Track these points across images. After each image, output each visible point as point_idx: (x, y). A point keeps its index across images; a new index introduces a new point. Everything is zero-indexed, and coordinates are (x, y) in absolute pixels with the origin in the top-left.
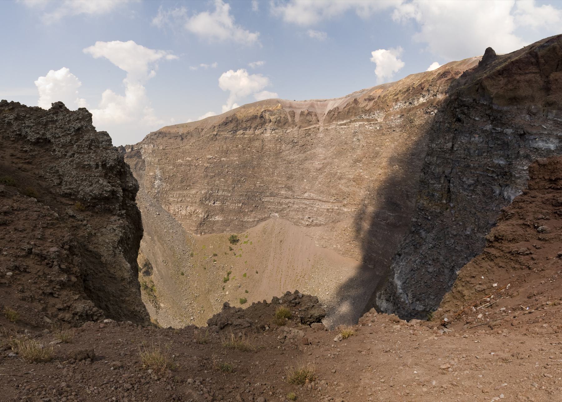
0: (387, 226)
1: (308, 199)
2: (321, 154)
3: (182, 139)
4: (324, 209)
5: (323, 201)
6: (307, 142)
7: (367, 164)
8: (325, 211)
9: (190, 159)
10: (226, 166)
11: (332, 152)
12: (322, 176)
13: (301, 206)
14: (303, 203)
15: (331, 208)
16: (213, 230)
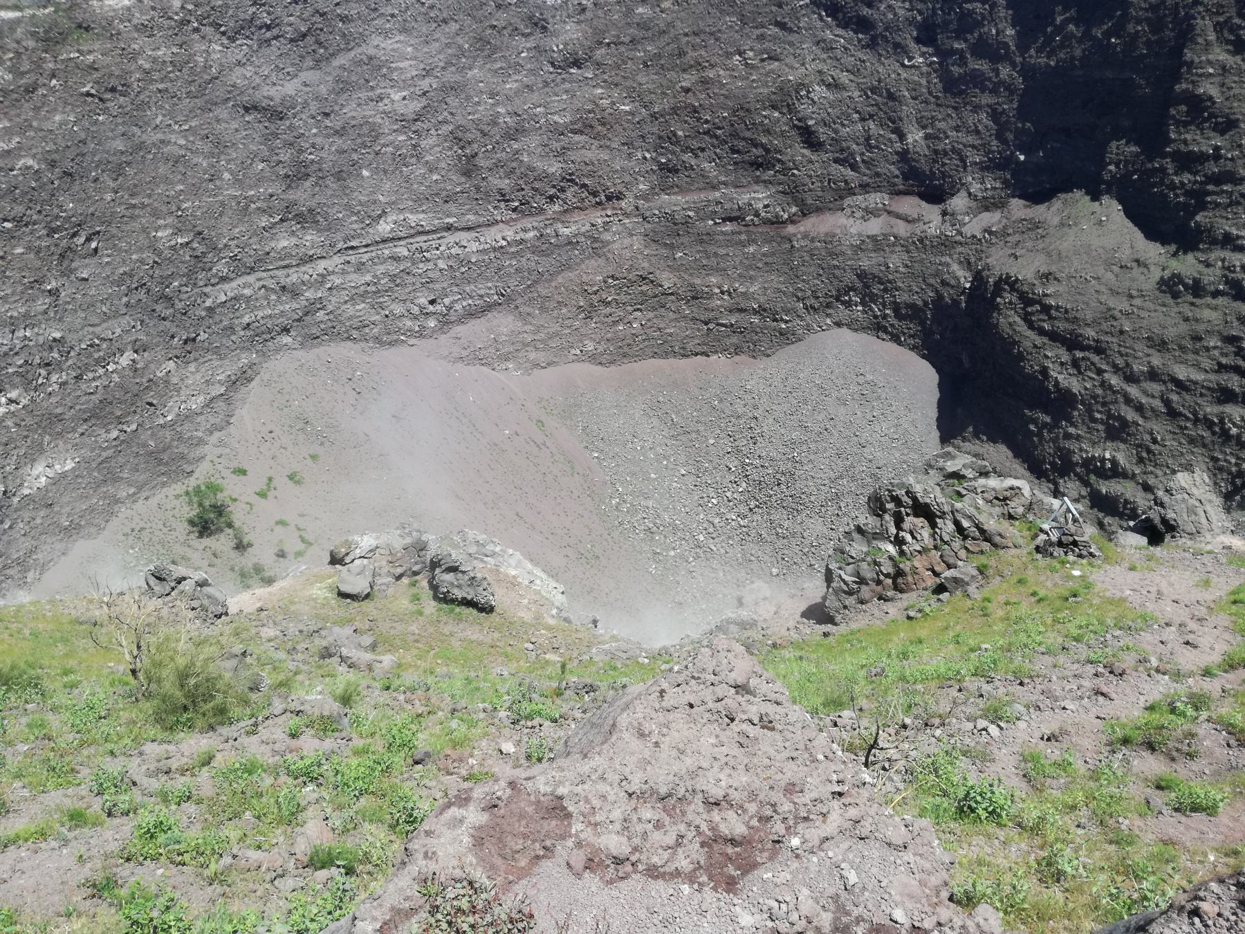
11: (448, 45)
12: (431, 142)
13: (381, 269)
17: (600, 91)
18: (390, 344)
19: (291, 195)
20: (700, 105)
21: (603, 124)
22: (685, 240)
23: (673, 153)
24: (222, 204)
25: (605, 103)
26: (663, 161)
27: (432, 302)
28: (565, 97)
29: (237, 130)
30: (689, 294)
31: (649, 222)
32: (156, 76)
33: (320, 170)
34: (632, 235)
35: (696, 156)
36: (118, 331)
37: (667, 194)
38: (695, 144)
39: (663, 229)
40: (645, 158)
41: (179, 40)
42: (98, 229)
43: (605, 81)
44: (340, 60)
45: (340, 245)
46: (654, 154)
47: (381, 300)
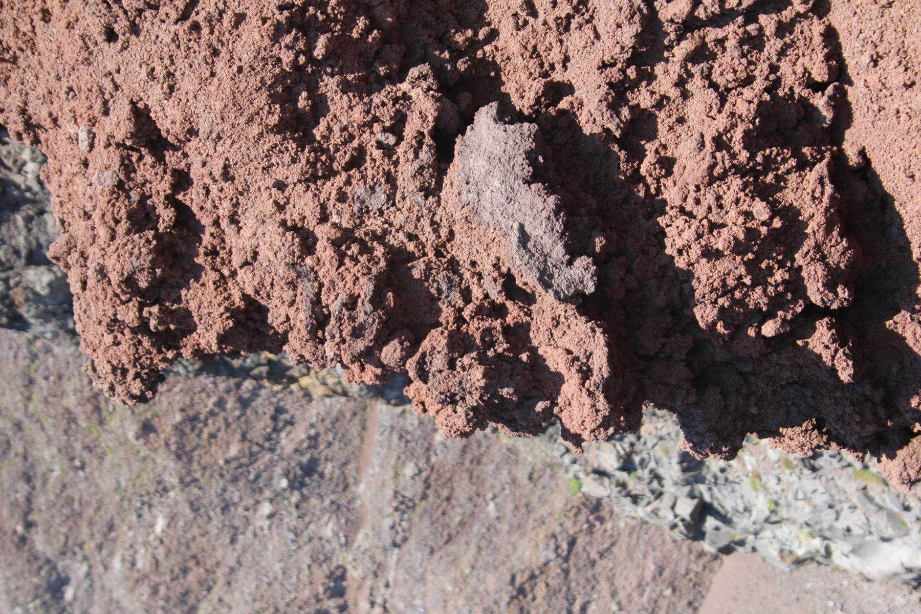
17: (117, 564)
20: (182, 410)
21: (185, 571)
23: (272, 464)
25: (143, 563)
26: (284, 483)
30: (582, 517)
31: (405, 540)
34: (422, 579)
35: (291, 423)
37: (357, 482)
38: (261, 426)
39: (426, 522)
40: (271, 516)
43: (100, 547)
46: (268, 493)
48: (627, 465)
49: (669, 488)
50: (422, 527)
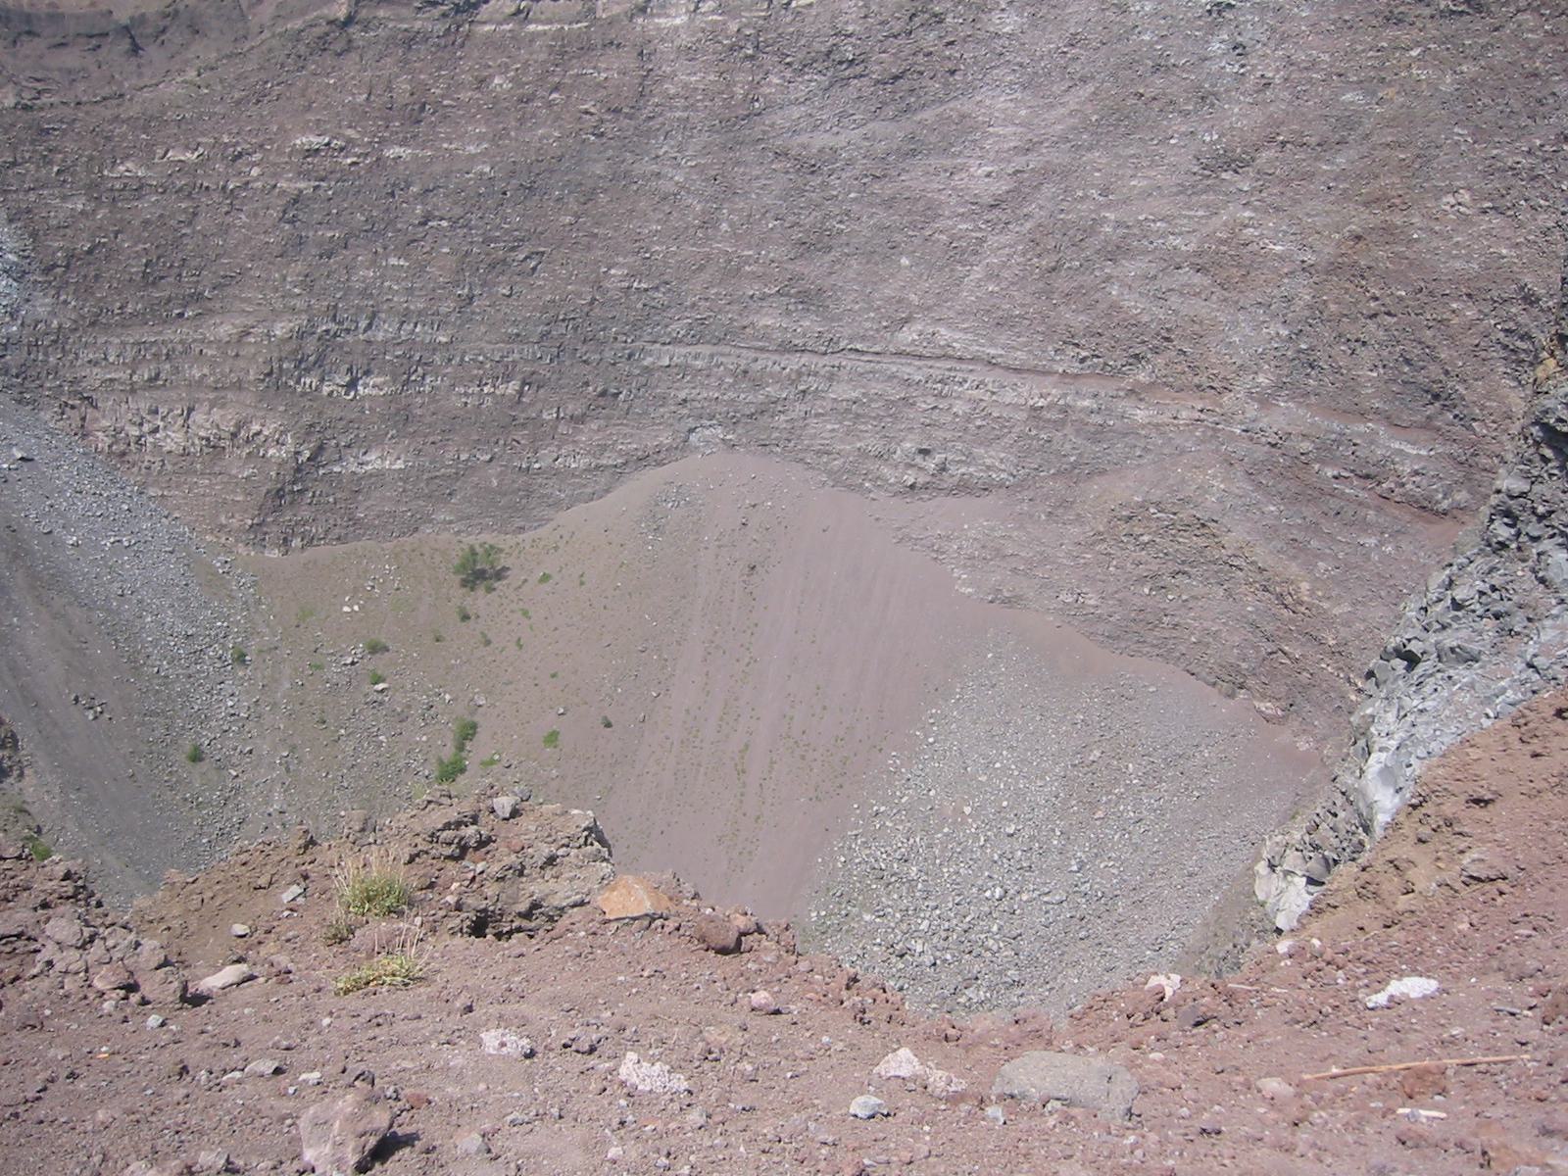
0: (1379, 509)
1: (920, 357)
2: (1009, 120)
3: (135, 49)
4: (1016, 407)
5: (1008, 368)
6: (920, 58)
7: (1286, 182)
8: (1022, 416)
9: (191, 156)
10: (414, 189)
12: (1004, 239)
13: (876, 388)
14: (893, 377)
15: (1049, 407)
16: (356, 522)
17: (1247, 214)
18: (850, 488)
19: (798, 267)
22: (1282, 487)
24: (708, 257)
26: (1304, 346)
27: (925, 452)
28: (1201, 213)
29: (757, 178)
32: (680, 103)
33: (848, 244)
36: (516, 356)
41: (723, 66)
42: (542, 249)
44: (928, 115)
45: (842, 345)
47: (862, 427)
48: (1457, 605)
49: (1433, 638)
50: (1261, 452)
